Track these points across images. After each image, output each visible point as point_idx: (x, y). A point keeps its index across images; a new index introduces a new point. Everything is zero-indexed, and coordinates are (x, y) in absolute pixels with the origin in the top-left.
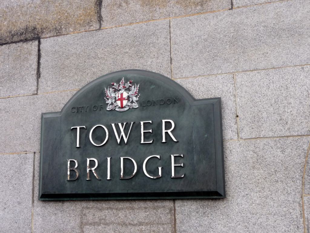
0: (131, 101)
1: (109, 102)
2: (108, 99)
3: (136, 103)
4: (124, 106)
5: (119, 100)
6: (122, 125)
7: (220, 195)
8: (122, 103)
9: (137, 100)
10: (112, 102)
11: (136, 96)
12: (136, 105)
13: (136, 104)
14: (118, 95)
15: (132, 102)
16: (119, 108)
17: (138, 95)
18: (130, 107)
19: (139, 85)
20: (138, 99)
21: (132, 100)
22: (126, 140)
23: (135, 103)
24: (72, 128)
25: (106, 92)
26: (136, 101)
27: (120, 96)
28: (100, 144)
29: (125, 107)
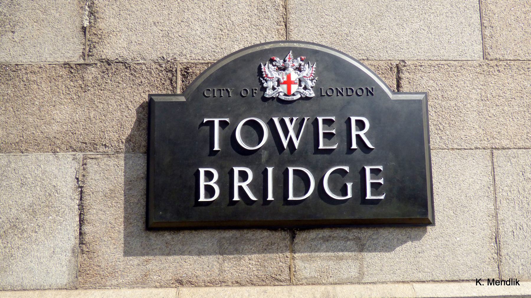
0: (303, 85)
1: (270, 84)
2: (266, 81)
3: (312, 90)
4: (292, 93)
5: (285, 83)
6: (291, 121)
7: (431, 223)
8: (289, 89)
9: (312, 85)
10: (273, 86)
11: (312, 80)
12: (311, 93)
13: (312, 92)
14: (283, 77)
15: (305, 88)
16: (285, 95)
17: (314, 79)
18: (302, 95)
19: (315, 65)
20: (314, 84)
21: (305, 86)
22: (296, 143)
23: (310, 90)
24: (205, 120)
25: (263, 70)
26: (312, 87)
27: (285, 77)
28: (255, 146)
29: (294, 95)
